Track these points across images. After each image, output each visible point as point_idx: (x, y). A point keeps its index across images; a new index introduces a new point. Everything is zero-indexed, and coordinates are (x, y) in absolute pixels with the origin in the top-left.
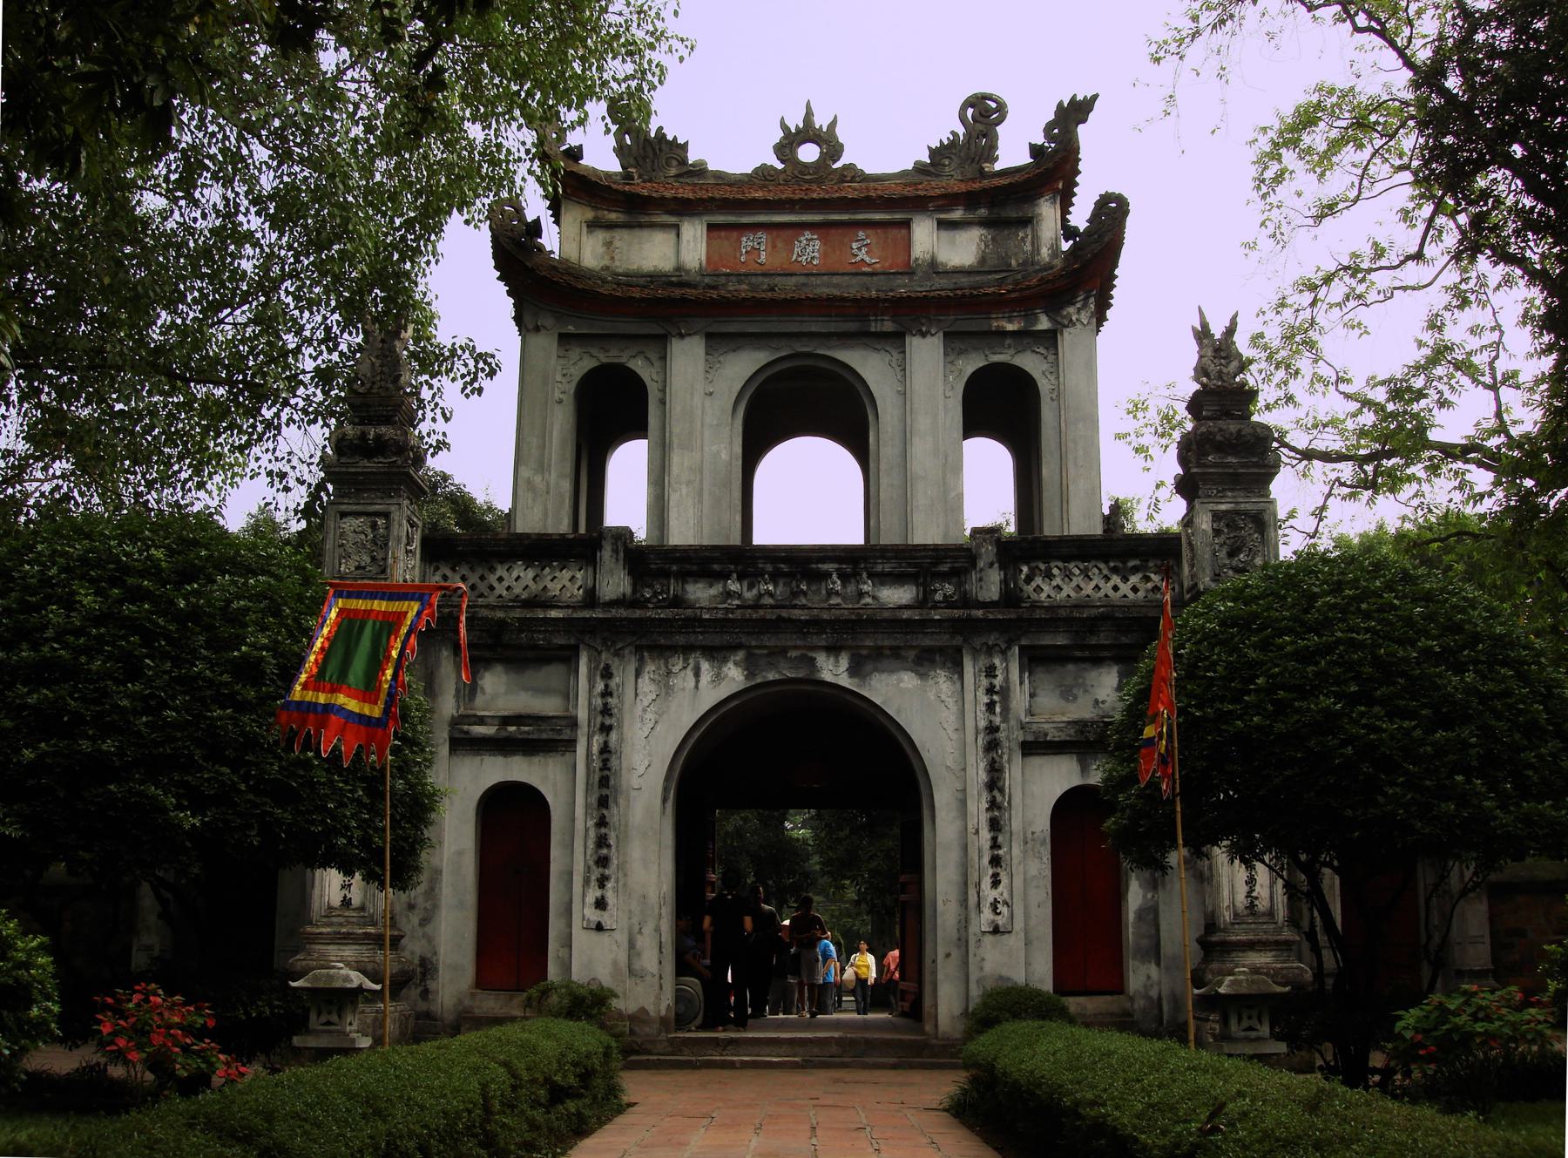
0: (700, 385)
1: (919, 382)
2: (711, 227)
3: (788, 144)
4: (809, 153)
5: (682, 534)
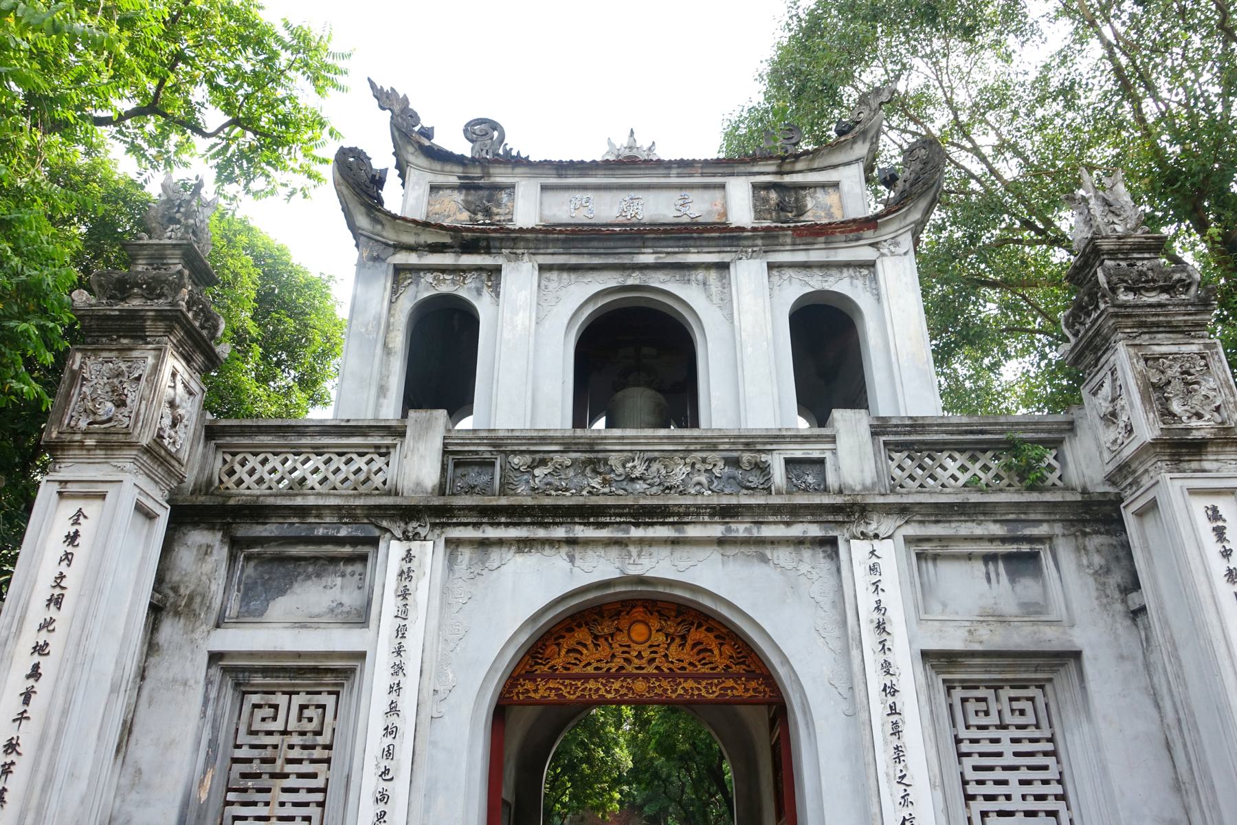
2: (544, 188)
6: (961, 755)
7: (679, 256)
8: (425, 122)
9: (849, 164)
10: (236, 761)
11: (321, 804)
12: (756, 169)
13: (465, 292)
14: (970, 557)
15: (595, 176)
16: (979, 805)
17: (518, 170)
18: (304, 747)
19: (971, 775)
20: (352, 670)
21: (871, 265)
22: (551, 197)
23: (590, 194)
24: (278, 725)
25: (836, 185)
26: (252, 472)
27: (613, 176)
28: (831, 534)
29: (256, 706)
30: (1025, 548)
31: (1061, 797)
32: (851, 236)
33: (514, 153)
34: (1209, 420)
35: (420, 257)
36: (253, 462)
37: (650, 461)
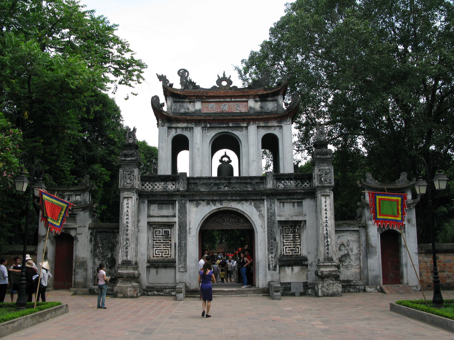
0: (200, 138)
1: (252, 137)
3: (219, 81)
4: (224, 83)
5: (197, 174)
6: (283, 238)
8: (171, 82)
10: (154, 240)
11: (171, 247)
14: (290, 202)
16: (285, 247)
18: (166, 238)
19: (285, 241)
20: (173, 225)
22: (204, 104)
23: (214, 104)
24: (161, 234)
29: (156, 231)
30: (300, 201)
31: (300, 245)
36: (147, 183)
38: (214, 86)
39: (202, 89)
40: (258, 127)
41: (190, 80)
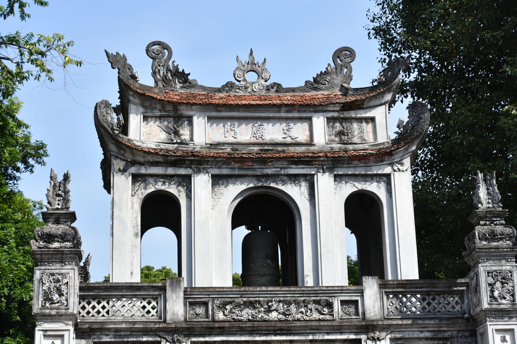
7: (286, 170)
9: (381, 105)
12: (329, 109)
13: (172, 189)
15: (238, 111)
17: (194, 107)
21: (388, 176)
25: (372, 120)
26: (94, 308)
27: (248, 111)
28: (358, 337)
32: (378, 159)
33: (181, 70)
34: (508, 300)
35: (146, 168)
36: (94, 303)
37: (280, 301)
38: (228, 83)
39: (203, 88)
40: (336, 176)
41: (176, 68)
